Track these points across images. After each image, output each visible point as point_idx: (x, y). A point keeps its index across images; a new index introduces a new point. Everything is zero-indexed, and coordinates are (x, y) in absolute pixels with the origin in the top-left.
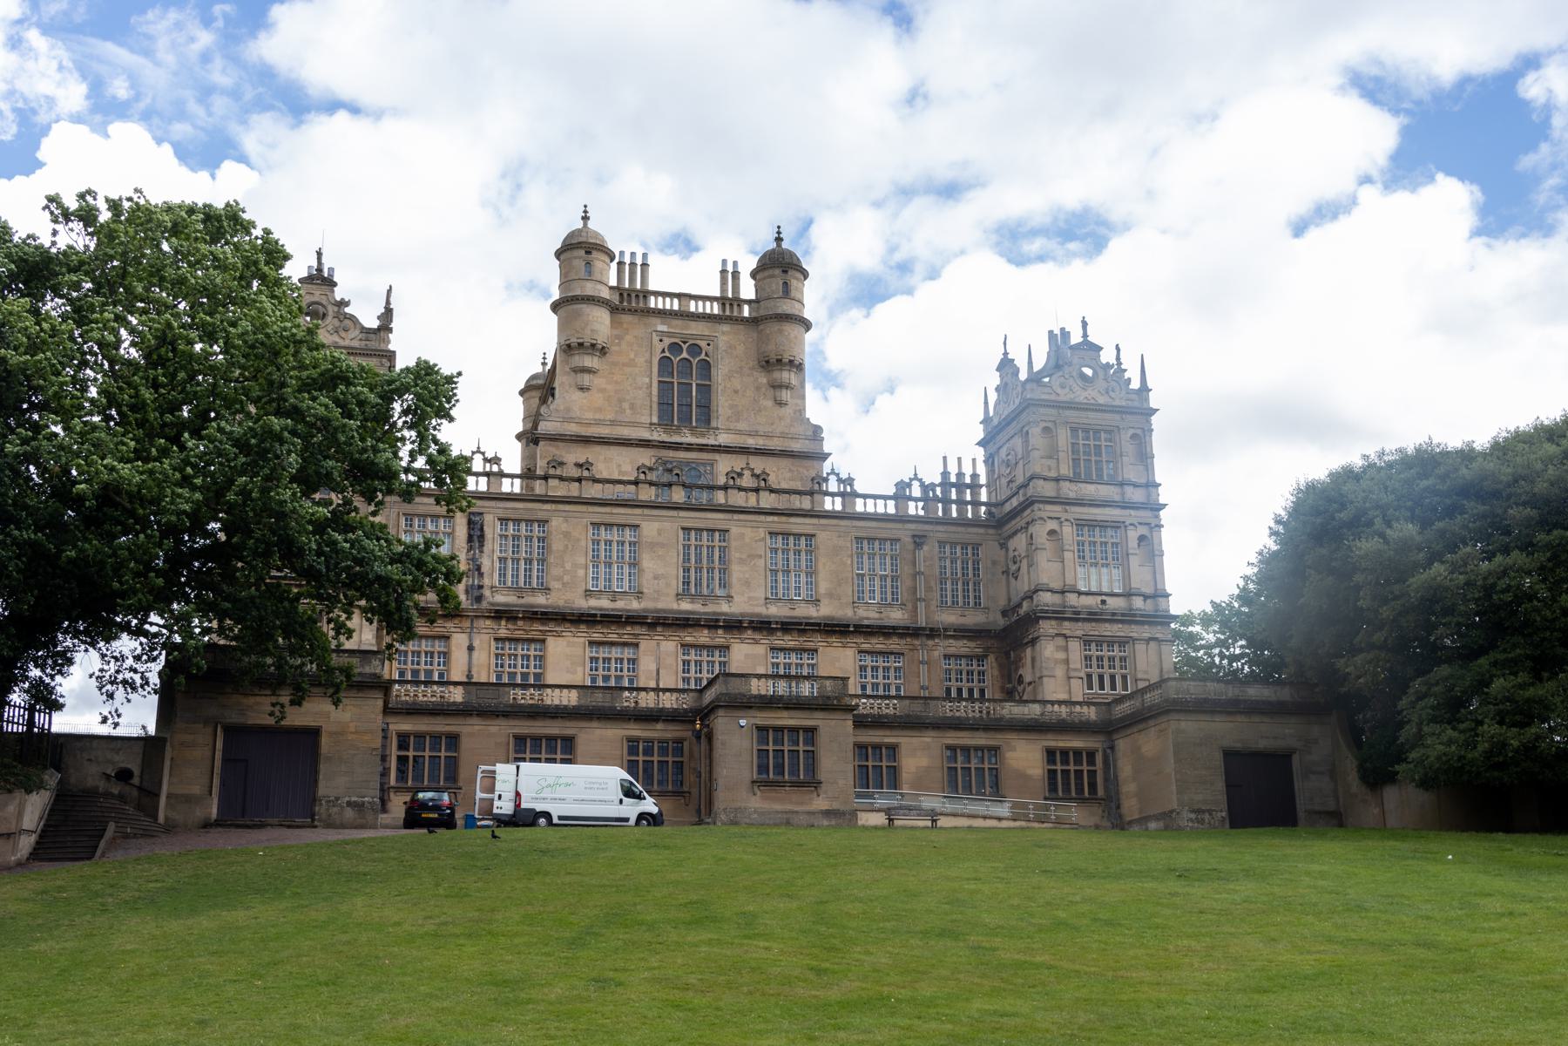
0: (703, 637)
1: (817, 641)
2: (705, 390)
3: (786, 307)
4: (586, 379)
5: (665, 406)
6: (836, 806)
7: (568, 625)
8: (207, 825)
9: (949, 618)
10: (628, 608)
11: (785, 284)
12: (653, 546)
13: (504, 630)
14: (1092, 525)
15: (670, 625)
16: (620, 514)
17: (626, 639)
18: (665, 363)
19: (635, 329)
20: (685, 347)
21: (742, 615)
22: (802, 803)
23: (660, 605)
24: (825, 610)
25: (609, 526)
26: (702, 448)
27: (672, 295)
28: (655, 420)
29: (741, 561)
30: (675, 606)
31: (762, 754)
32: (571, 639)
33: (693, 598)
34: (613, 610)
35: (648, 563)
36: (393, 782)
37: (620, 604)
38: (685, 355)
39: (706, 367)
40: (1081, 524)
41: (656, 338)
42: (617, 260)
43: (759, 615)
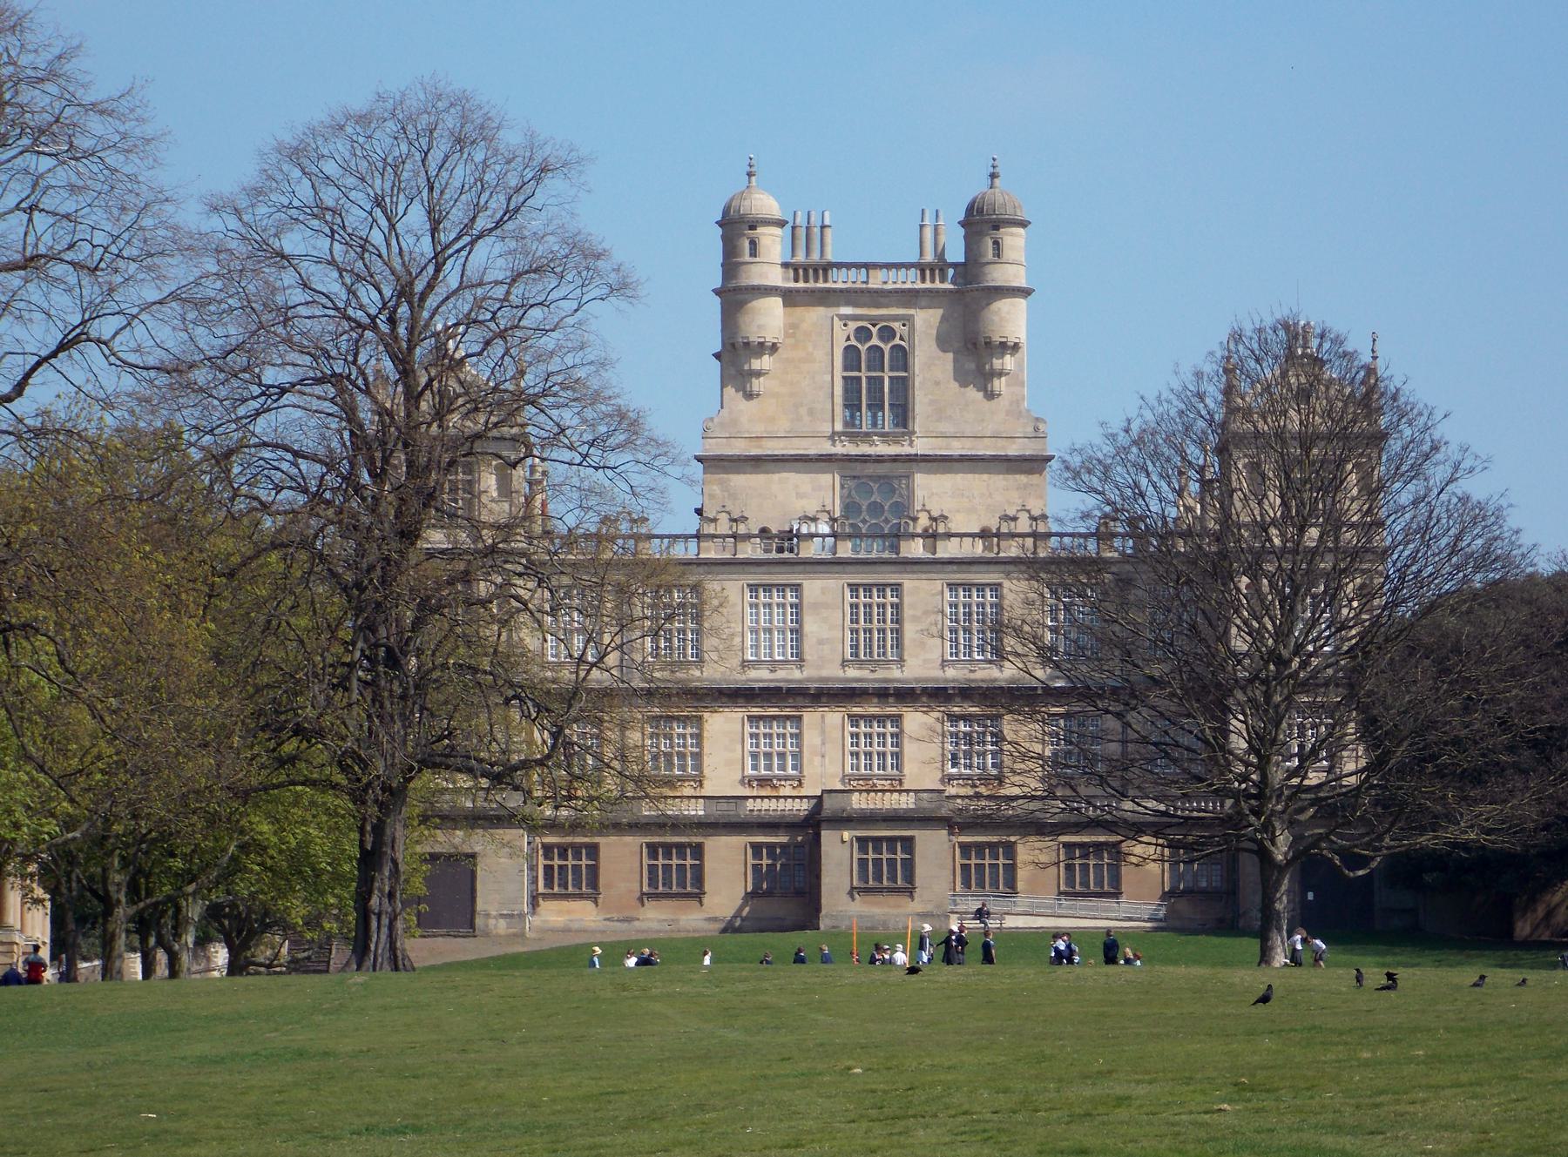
5: (852, 404)
6: (929, 908)
7: (725, 700)
10: (790, 677)
11: (996, 243)
12: (816, 606)
15: (835, 695)
17: (787, 712)
18: (851, 355)
20: (874, 330)
21: (917, 680)
22: (899, 907)
23: (825, 673)
25: (768, 588)
26: (895, 459)
27: (858, 266)
28: (839, 427)
29: (915, 619)
30: (840, 673)
31: (863, 863)
32: (729, 715)
33: (861, 664)
34: (772, 681)
35: (811, 626)
36: (541, 889)
37: (781, 674)
38: (875, 341)
41: (838, 323)
42: (791, 224)
43: (936, 680)
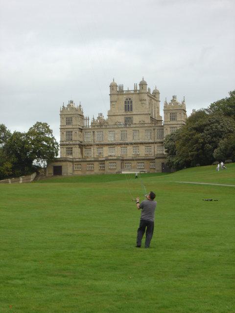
0: (124, 146)
1: (139, 145)
2: (131, 106)
3: (143, 91)
4: (114, 106)
5: (126, 110)
8: (31, 182)
9: (159, 140)
13: (98, 147)
14: (173, 127)
16: (112, 130)
18: (125, 102)
19: (120, 97)
24: (141, 141)
26: (131, 115)
35: (116, 136)
39: (131, 102)
40: (171, 127)
